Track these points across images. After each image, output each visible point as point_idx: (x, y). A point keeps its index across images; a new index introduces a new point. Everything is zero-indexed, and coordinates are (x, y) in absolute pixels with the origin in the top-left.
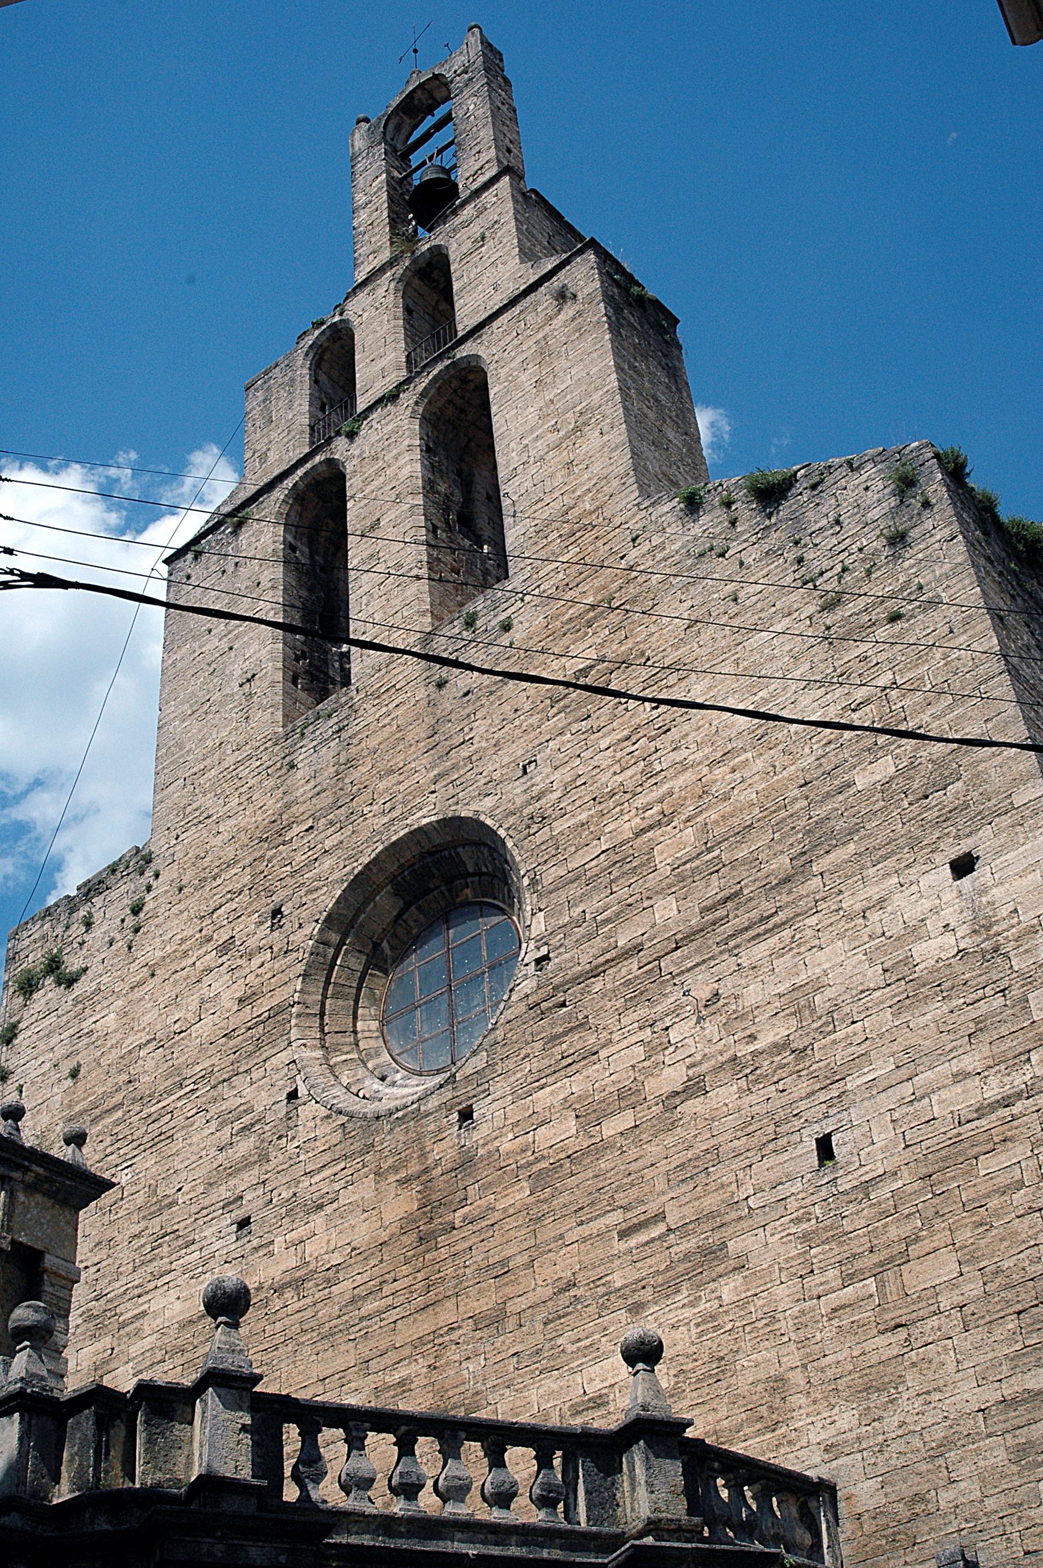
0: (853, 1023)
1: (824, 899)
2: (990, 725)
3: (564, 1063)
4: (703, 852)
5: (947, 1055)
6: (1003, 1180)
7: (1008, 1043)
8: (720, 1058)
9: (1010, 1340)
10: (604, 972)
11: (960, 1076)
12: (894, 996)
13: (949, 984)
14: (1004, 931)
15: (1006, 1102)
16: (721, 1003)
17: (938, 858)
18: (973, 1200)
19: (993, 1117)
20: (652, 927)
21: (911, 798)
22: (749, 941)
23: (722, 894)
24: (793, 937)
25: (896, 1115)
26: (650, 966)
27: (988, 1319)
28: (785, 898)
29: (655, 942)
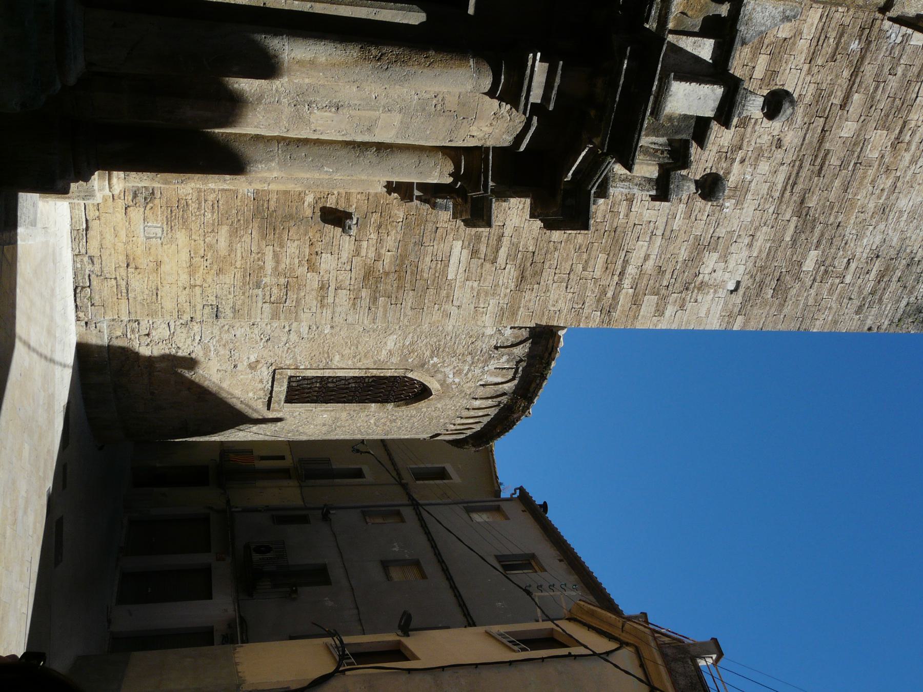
0: (708, 215)
1: (776, 219)
2: (782, 316)
3: (822, 38)
4: (858, 160)
5: (660, 255)
6: (592, 263)
7: (645, 282)
8: (747, 140)
9: (526, 246)
10: (850, 80)
11: (647, 258)
12: (704, 239)
13: (690, 265)
14: (692, 295)
15: (622, 274)
16: (774, 148)
17: (746, 277)
18: (592, 248)
19: (620, 267)
20: (847, 118)
21: (784, 273)
22: (791, 173)
23: (826, 165)
24: (772, 197)
25: (652, 224)
26: (827, 111)
27: (539, 239)
28: (794, 198)
29: (838, 118)
